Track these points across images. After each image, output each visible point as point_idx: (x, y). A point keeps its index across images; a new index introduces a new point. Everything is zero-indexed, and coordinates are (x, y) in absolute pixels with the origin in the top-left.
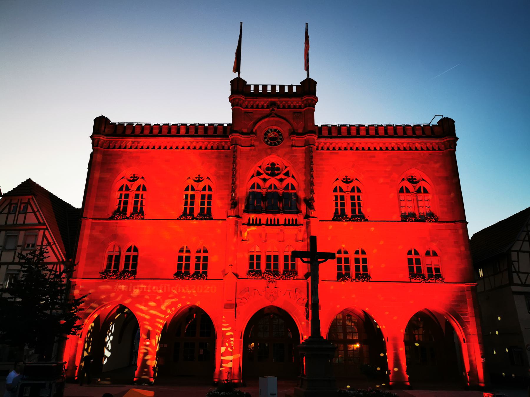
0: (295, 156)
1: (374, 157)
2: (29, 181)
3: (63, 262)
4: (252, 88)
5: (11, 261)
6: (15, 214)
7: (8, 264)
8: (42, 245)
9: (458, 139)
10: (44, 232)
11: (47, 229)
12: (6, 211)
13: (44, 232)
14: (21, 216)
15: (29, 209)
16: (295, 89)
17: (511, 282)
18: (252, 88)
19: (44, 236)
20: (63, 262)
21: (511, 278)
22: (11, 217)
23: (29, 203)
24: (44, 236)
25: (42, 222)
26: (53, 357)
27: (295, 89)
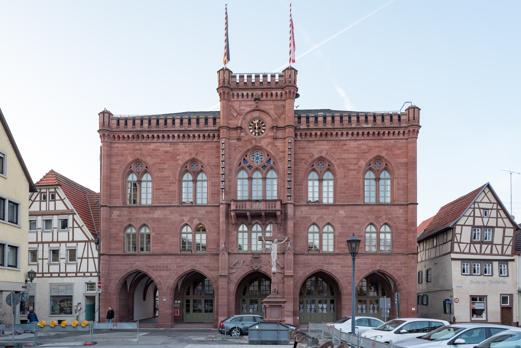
0: (277, 146)
1: (346, 145)
2: (52, 171)
3: (92, 241)
4: (238, 78)
5: (51, 240)
6: (46, 201)
7: (49, 243)
8: (73, 228)
9: (420, 127)
10: (73, 217)
11: (75, 214)
12: (38, 199)
13: (73, 217)
14: (52, 204)
15: (57, 197)
16: (277, 77)
17: (452, 251)
18: (238, 78)
19: (74, 220)
20: (92, 241)
21: (452, 247)
22: (43, 204)
23: (56, 192)
24: (74, 220)
25: (70, 208)
26: (96, 310)
27: (277, 77)
